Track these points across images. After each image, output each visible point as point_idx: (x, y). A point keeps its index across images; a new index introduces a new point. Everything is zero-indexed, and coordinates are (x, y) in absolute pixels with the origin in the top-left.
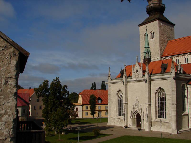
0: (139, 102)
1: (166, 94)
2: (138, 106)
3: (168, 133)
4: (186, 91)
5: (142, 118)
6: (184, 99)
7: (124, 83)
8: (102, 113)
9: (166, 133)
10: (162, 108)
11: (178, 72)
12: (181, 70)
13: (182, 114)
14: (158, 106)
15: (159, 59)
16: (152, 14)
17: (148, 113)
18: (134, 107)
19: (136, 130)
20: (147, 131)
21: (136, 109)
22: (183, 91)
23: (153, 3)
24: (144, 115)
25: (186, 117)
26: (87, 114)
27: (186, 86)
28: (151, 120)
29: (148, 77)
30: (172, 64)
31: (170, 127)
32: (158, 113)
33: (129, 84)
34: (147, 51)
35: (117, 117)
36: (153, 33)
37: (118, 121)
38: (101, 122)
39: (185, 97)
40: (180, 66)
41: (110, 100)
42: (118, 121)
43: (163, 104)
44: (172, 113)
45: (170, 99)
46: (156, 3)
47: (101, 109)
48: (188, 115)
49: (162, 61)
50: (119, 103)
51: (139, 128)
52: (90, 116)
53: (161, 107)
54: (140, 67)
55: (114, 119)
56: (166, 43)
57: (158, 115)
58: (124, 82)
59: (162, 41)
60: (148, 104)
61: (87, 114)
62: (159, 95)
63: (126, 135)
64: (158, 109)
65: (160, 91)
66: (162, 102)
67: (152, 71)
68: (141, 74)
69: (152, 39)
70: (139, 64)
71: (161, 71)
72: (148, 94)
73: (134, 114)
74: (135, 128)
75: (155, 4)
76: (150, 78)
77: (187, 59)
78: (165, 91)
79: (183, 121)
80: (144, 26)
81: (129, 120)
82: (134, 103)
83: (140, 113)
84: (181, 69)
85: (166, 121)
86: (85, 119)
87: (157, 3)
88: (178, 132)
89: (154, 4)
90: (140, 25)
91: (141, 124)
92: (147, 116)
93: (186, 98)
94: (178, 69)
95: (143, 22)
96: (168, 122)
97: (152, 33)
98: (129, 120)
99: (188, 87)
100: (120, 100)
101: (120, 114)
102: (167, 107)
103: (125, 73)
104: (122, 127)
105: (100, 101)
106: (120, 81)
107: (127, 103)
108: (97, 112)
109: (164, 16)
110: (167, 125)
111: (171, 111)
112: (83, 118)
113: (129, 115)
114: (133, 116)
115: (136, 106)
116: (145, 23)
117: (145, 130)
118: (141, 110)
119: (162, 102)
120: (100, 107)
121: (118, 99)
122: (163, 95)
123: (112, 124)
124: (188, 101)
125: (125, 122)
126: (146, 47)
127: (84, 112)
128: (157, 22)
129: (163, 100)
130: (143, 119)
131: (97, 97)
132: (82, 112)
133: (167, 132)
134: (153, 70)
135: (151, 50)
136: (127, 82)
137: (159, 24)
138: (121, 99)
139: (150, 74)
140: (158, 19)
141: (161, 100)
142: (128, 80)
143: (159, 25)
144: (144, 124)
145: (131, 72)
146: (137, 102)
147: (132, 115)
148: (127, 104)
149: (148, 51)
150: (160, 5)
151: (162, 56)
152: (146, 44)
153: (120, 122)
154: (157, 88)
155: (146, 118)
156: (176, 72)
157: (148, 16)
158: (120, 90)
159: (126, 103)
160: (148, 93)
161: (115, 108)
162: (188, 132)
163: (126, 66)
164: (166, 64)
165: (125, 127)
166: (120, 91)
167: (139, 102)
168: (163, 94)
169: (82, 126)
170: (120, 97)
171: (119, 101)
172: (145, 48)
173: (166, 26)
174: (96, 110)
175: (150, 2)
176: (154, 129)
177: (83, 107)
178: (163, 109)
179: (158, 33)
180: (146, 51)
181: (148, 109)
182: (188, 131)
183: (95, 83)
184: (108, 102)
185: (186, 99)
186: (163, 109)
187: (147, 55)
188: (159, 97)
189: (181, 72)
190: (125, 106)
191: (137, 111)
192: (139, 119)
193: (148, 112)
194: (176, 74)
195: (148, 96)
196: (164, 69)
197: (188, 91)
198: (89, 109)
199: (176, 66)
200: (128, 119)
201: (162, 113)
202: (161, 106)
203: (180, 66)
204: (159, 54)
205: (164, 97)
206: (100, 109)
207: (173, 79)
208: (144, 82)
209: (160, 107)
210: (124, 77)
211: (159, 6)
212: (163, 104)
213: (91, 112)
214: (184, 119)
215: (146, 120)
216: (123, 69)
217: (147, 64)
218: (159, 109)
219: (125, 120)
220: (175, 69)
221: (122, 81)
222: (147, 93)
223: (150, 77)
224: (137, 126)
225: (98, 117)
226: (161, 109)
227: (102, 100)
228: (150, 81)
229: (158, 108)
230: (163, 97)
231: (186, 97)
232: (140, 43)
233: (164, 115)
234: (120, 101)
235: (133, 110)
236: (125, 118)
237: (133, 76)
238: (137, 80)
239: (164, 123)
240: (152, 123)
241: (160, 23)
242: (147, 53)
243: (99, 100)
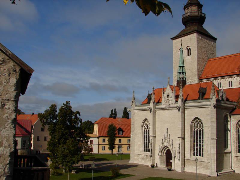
0: (170, 135)
1: (204, 125)
2: (169, 140)
3: (205, 175)
4: (229, 123)
5: (173, 155)
6: (226, 132)
7: (152, 111)
8: (123, 148)
9: (203, 174)
10: (199, 143)
11: (220, 98)
12: (223, 96)
13: (224, 152)
14: (193, 141)
15: (196, 82)
16: (188, 25)
17: (181, 149)
18: (163, 141)
19: (165, 171)
20: (179, 172)
21: (166, 144)
22: (225, 122)
23: (191, 11)
24: (175, 152)
25: (229, 155)
26: (104, 148)
27: (229, 116)
28: (185, 158)
29: (182, 104)
30: (212, 89)
31: (209, 167)
32: (193, 149)
33: (158, 112)
34: (181, 71)
35: (142, 153)
36: (190, 48)
37: (143, 158)
38: (122, 159)
39: (227, 131)
40: (222, 91)
41: (134, 131)
42: (143, 158)
43: (200, 138)
44: (211, 150)
45: (209, 132)
46: (195, 12)
47: (122, 143)
48: (231, 152)
49: (200, 85)
50: (145, 135)
51: (169, 167)
52: (107, 151)
53: (197, 142)
54: (172, 91)
55: (138, 156)
56: (205, 62)
57: (193, 153)
58: (151, 110)
59: (201, 59)
60: (182, 138)
61: (104, 148)
62: (194, 127)
63: (153, 176)
64: (194, 144)
65: (197, 121)
66: (198, 136)
67: (187, 97)
68: (173, 100)
69: (188, 57)
70: (171, 87)
71: (198, 96)
72: (182, 126)
73: (163, 150)
74: (164, 167)
75: (193, 12)
76: (185, 106)
77: (232, 82)
78: (203, 122)
79: (224, 160)
80: (178, 40)
81: (157, 157)
82: (164, 136)
83: (170, 149)
84: (223, 95)
85: (203, 160)
86: (101, 154)
87: (196, 12)
88: (218, 174)
89: (192, 12)
90: (174, 39)
91: (171, 163)
92: (180, 153)
93: (228, 132)
94: (220, 95)
95: (178, 35)
96: (206, 161)
97: (188, 49)
98: (157, 157)
99: (231, 117)
100: (146, 132)
101: (146, 149)
102: (204, 142)
103: (153, 97)
104: (148, 166)
105: (121, 133)
106: (146, 107)
107: (154, 136)
108: (117, 147)
109: (204, 29)
110: (204, 164)
111: (209, 148)
113: (157, 151)
114: (161, 153)
115: (166, 140)
116: (180, 36)
117: (177, 171)
118: (172, 145)
119: (198, 136)
120: (121, 140)
121: (144, 130)
122: (200, 127)
123: (136, 162)
124: (231, 136)
125: (152, 160)
126: (181, 67)
127: (100, 145)
128: (194, 36)
129: (200, 134)
130: (175, 157)
131: (118, 127)
132: (98, 145)
133: (204, 173)
134: (188, 95)
135: (187, 70)
136: (156, 109)
137: (197, 37)
138: (147, 130)
139: (184, 100)
141: (197, 134)
142: (157, 107)
143: (197, 39)
144: (176, 162)
145: (161, 98)
146: (167, 135)
147: (161, 151)
148: (154, 137)
149: (182, 71)
150: (199, 14)
151: (200, 79)
152: (181, 62)
153: (145, 159)
154: (193, 118)
155: (178, 155)
156: (216, 98)
157: (184, 27)
158: (146, 120)
159: (153, 136)
160: (182, 123)
161: (140, 142)
162: (231, 174)
163: (154, 90)
164: (205, 88)
165: (151, 166)
166: (146, 121)
167: (170, 135)
168: (200, 125)
169: (98, 164)
170: (147, 128)
171: (145, 134)
172: (179, 67)
173: (205, 40)
174: (115, 144)
175: (187, 10)
176: (188, 169)
177: (99, 139)
178: (200, 145)
179: (196, 48)
180: (180, 71)
181: (181, 144)
182: (231, 173)
183: (115, 109)
184: (131, 134)
185: (229, 133)
186: (200, 145)
187: (181, 76)
188: (195, 130)
189: (223, 99)
190: (152, 140)
191: (166, 146)
192: (169, 156)
193: (180, 147)
194: (217, 100)
195: (182, 128)
196: (202, 94)
197: (231, 123)
198: (107, 142)
199: (217, 90)
200: (155, 156)
201: (198, 150)
202: (197, 141)
203: (222, 91)
204: (197, 75)
205: (201, 130)
206: (121, 142)
207: (213, 107)
208: (177, 110)
209: (196, 143)
210: (152, 103)
211: (197, 16)
212: (200, 138)
213: (109, 146)
214: (226, 158)
215: (178, 158)
216: (150, 93)
217: (181, 88)
218: (194, 145)
219: (152, 158)
220: (215, 95)
221: (150, 108)
222: (180, 123)
223: (185, 104)
224: (167, 165)
225: (118, 153)
226: (197, 145)
227: (123, 131)
228: (185, 108)
229: (193, 143)
230: (200, 130)
231: (229, 131)
232: (173, 62)
233: (201, 152)
234: (146, 134)
235: (162, 145)
236: (151, 155)
237: (163, 102)
238: (169, 107)
239: (200, 162)
240: (185, 162)
241: (199, 37)
242: (182, 73)
243: (120, 131)
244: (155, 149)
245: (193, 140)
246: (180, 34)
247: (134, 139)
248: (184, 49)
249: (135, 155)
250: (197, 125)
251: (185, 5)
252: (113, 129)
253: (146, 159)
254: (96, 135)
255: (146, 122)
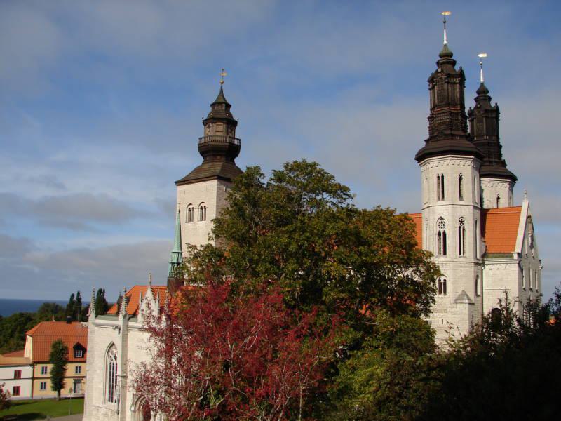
7: (121, 331)
34: (176, 262)
37: (106, 415)
38: (71, 414)
41: (91, 364)
50: (110, 372)
52: (50, 393)
58: (120, 330)
61: (43, 386)
87: (221, 136)
95: (188, 176)
105: (79, 353)
112: (34, 398)
127: (35, 381)
128: (214, 183)
132: (31, 381)
140: (216, 177)
142: (131, 324)
145: (138, 309)
149: (178, 260)
157: (199, 160)
158: (112, 345)
171: (110, 369)
177: (34, 368)
183: (79, 294)
198: (49, 375)
206: (80, 372)
236: (118, 410)
241: (222, 186)
243: (78, 350)
244: (125, 399)
246: (193, 177)
247: (93, 379)
248: (196, 206)
249: (93, 407)
251: (205, 119)
252: (63, 349)
253: (111, 416)
254: (29, 358)
255: (113, 349)
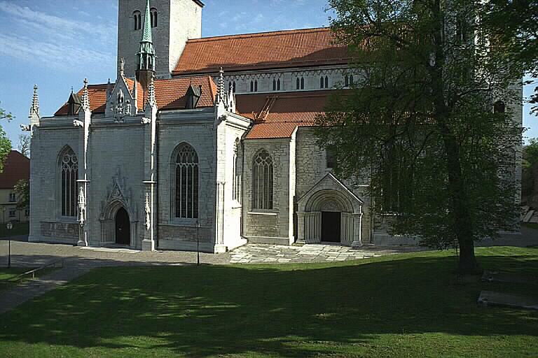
43: (190, 183)
118: (131, 198)
121: (61, 171)
129: (190, 175)
141: (184, 175)
161: (53, 196)
171: (63, 178)
202: (184, 188)
245: (174, 186)
250: (184, 158)
